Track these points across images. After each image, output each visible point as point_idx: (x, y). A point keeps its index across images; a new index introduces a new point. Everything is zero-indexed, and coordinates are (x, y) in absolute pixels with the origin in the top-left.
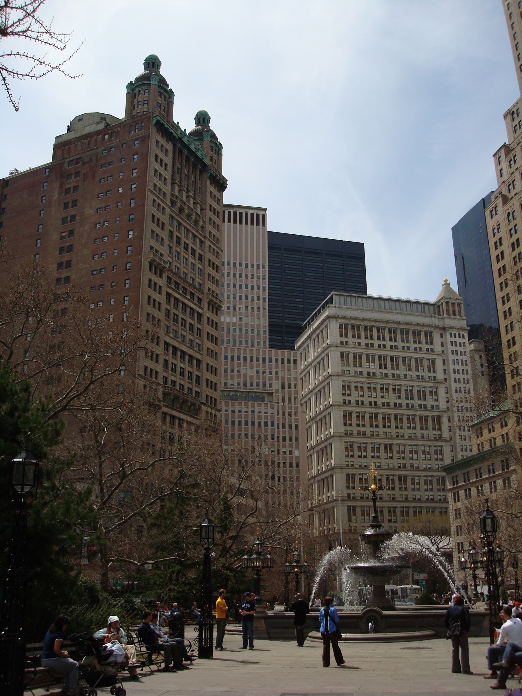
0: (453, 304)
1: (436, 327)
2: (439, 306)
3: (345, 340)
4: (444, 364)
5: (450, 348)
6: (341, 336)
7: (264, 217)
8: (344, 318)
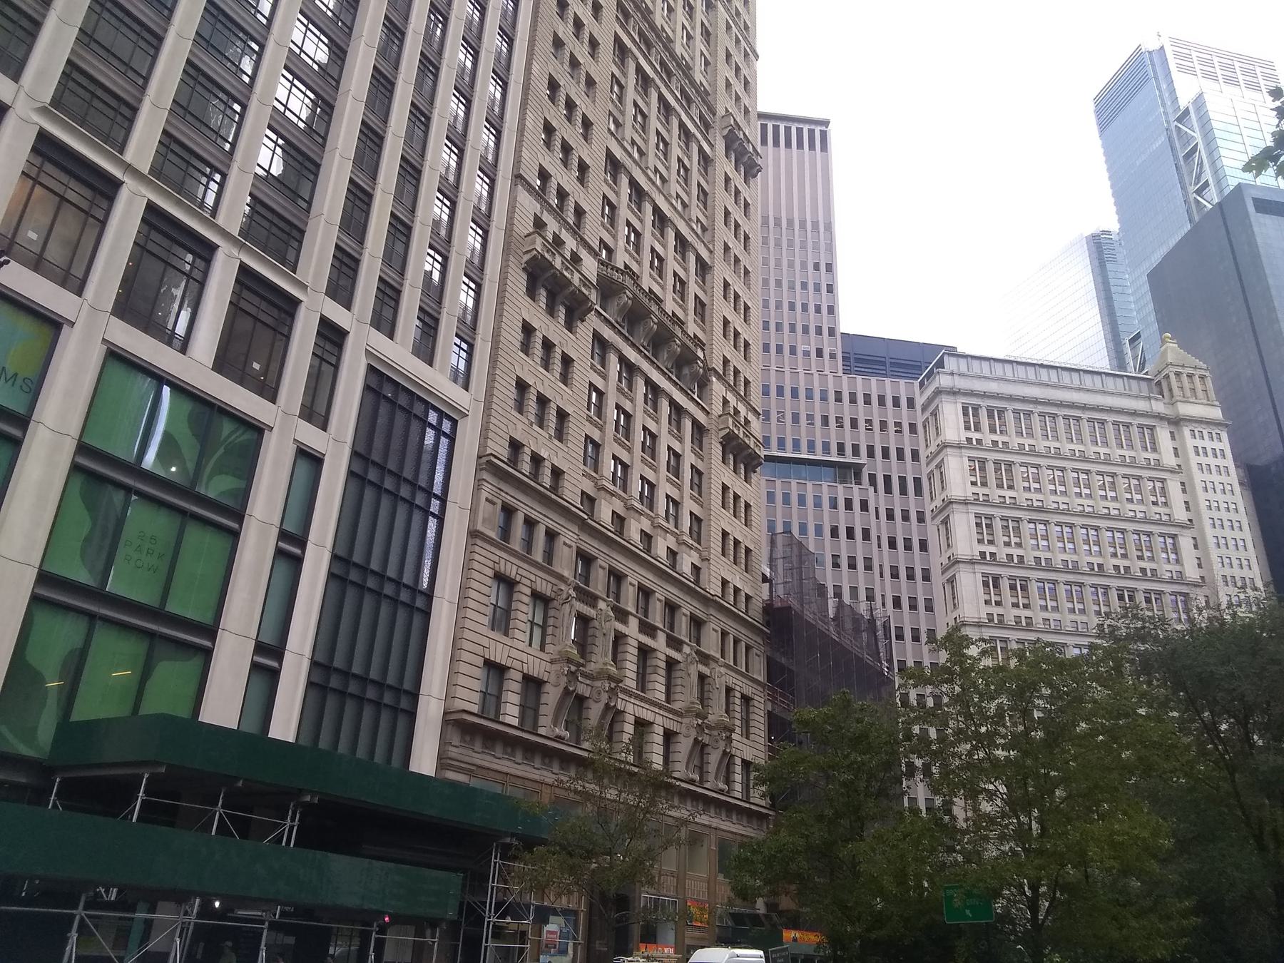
0: (1190, 376)
1: (1160, 417)
2: (1159, 383)
3: (975, 436)
4: (1184, 491)
5: (1194, 460)
6: (967, 428)
7: (824, 135)
8: (971, 394)
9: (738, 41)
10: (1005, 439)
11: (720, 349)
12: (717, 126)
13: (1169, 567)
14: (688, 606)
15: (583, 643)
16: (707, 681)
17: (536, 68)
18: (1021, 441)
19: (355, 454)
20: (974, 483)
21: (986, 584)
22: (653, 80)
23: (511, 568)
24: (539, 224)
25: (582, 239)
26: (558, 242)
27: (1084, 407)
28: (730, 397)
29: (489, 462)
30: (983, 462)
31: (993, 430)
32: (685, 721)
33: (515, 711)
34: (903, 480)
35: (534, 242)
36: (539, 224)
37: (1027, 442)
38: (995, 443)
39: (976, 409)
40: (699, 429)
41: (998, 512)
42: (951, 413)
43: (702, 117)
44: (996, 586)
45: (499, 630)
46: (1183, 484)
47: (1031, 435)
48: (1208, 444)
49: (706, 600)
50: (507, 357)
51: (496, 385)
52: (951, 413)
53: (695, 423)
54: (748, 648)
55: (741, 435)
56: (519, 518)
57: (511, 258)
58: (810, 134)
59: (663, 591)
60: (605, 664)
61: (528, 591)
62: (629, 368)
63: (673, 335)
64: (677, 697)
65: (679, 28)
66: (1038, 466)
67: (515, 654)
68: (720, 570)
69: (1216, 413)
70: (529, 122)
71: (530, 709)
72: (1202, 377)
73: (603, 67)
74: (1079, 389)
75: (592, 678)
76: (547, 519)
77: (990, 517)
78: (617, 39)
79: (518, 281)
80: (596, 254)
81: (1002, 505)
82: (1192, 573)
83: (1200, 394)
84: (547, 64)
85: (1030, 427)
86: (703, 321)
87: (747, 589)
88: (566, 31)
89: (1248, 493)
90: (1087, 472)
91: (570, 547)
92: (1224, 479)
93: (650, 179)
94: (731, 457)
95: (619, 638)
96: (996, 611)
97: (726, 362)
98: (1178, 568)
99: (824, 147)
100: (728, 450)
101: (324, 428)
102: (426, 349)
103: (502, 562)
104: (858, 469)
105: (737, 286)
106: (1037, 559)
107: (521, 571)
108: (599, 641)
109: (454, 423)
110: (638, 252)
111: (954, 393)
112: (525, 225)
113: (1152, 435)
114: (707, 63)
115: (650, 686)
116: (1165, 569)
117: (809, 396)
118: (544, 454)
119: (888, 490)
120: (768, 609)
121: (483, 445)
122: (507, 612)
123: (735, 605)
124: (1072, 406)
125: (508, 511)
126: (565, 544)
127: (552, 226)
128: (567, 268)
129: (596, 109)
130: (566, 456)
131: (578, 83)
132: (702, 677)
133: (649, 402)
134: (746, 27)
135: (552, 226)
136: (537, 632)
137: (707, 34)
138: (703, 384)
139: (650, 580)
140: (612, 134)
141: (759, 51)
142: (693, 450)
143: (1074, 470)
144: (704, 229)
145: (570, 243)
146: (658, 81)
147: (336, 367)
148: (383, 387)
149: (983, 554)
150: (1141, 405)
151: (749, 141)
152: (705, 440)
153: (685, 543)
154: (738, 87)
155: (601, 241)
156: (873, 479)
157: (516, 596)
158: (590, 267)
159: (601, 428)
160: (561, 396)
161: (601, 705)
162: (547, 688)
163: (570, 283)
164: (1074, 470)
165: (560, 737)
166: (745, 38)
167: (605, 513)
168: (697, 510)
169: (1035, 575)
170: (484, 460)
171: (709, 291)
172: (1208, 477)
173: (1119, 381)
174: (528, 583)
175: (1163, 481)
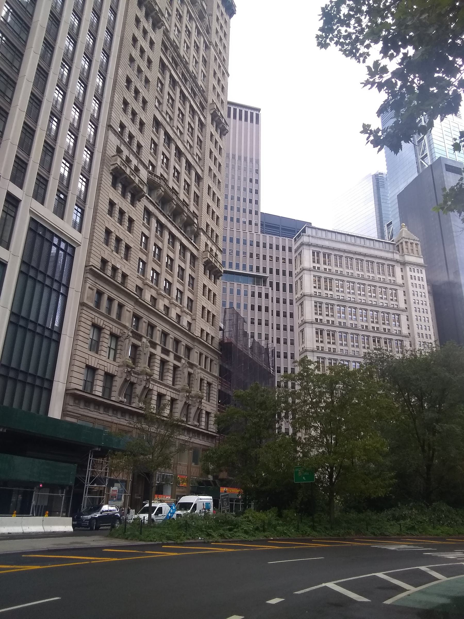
0: (412, 244)
1: (397, 261)
2: (398, 246)
3: (317, 265)
4: (405, 295)
5: (410, 281)
6: (314, 262)
7: (258, 116)
8: (317, 246)
9: (220, 66)
10: (330, 268)
11: (205, 220)
12: (208, 108)
13: (395, 328)
14: (185, 341)
15: (134, 358)
16: (192, 376)
17: (120, 72)
18: (337, 269)
19: (23, 262)
20: (315, 287)
21: (317, 333)
22: (178, 82)
23: (100, 322)
24: (119, 151)
25: (140, 160)
26: (128, 160)
27: (365, 255)
28: (209, 243)
29: (91, 269)
30: (320, 278)
31: (325, 263)
32: (181, 394)
33: (100, 389)
34: (284, 285)
35: (116, 160)
36: (119, 151)
37: (339, 269)
38: (325, 269)
39: (318, 253)
40: (193, 257)
41: (324, 301)
42: (307, 254)
43: (201, 103)
44: (321, 334)
45: (93, 351)
46: (404, 292)
47: (341, 266)
48: (417, 275)
49: (194, 339)
50: (101, 217)
51: (95, 231)
52: (307, 254)
53: (192, 254)
54: (211, 361)
55: (213, 261)
56: (105, 297)
57: (105, 167)
58: (251, 115)
59: (173, 334)
60: (145, 368)
61: (109, 333)
62: (161, 226)
63: (183, 211)
64: (178, 383)
65: (192, 57)
66: (343, 281)
67: (101, 362)
68: (201, 325)
69: (421, 261)
70: (116, 99)
71: (108, 388)
72: (417, 244)
73: (154, 74)
74: (364, 247)
75: (138, 374)
76: (119, 298)
77: (321, 303)
78: (161, 60)
79: (108, 179)
80: (147, 168)
81: (326, 298)
82: (405, 331)
83: (415, 252)
84: (126, 71)
85: (341, 263)
86: (198, 205)
87: (212, 334)
88: (136, 54)
89: (431, 298)
90: (364, 284)
91: (130, 312)
92: (422, 290)
93: (175, 132)
94: (208, 271)
95: (152, 355)
96: (320, 345)
97: (208, 225)
98: (399, 329)
99: (257, 122)
100: (207, 268)
101: (8, 248)
102: (60, 210)
103: (96, 318)
104: (265, 279)
105: (214, 188)
106: (340, 323)
107: (105, 323)
108: (142, 357)
109: (74, 249)
110: (167, 168)
111: (309, 245)
112: (112, 151)
113: (393, 269)
114: (204, 76)
115: (165, 378)
116: (394, 329)
117: (245, 243)
118: (118, 266)
119: (278, 289)
120: (221, 343)
121: (88, 261)
122: (98, 342)
123: (206, 341)
124: (360, 254)
125: (100, 294)
126: (127, 310)
127: (126, 152)
128: (133, 174)
129: (149, 95)
130: (129, 268)
131: (141, 81)
132: (190, 374)
133: (170, 243)
134: (224, 60)
135: (126, 152)
136: (112, 352)
137: (205, 61)
138: (197, 236)
139: (167, 329)
140: (157, 108)
141: (229, 72)
142: (190, 268)
143: (359, 283)
144: (200, 159)
145: (134, 162)
146: (180, 83)
147: (14, 218)
148: (38, 230)
149: (317, 319)
150: (389, 256)
151: (223, 117)
152: (196, 263)
153: (185, 312)
154: (219, 89)
155: (150, 161)
156: (271, 284)
157: (102, 335)
158: (144, 174)
159: (147, 255)
160: (127, 238)
161: (142, 387)
162: (116, 378)
163: (134, 182)
164: (359, 283)
165: (121, 401)
166: (223, 66)
167: (147, 296)
168: (191, 296)
169: (338, 329)
170: (88, 268)
171: (201, 190)
172: (415, 289)
173: (381, 244)
174: (109, 328)
175: (396, 290)
